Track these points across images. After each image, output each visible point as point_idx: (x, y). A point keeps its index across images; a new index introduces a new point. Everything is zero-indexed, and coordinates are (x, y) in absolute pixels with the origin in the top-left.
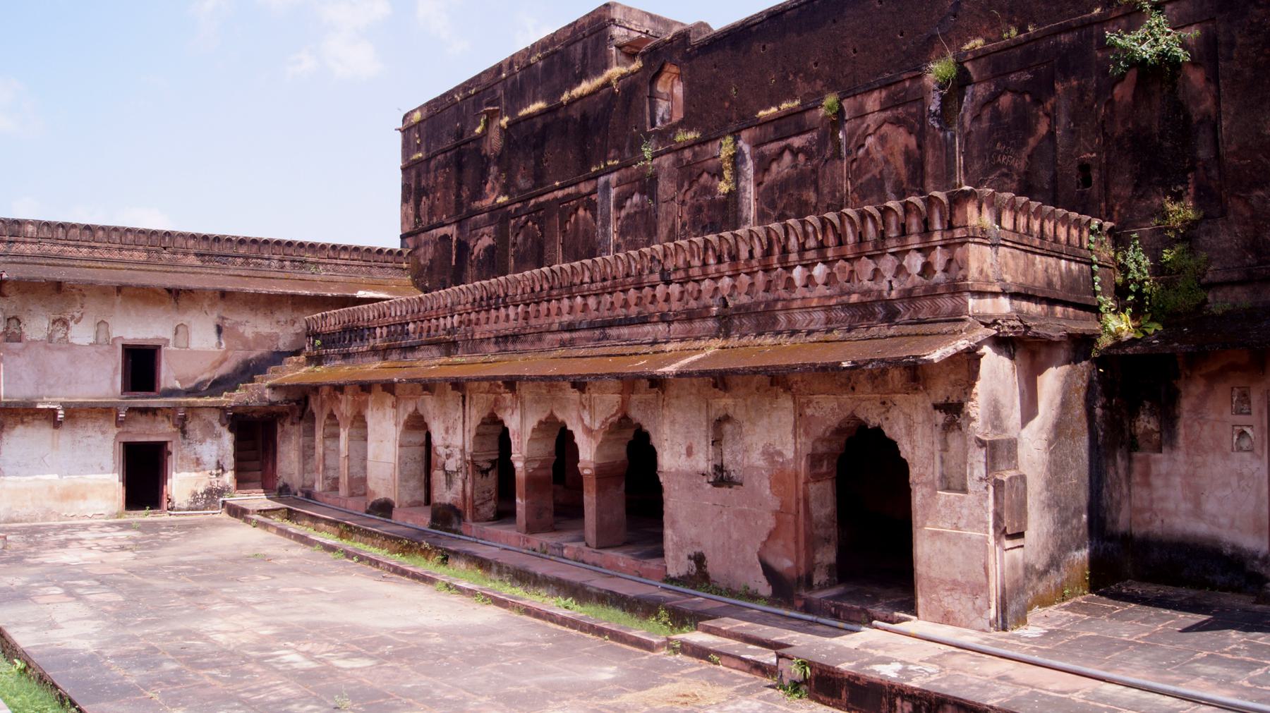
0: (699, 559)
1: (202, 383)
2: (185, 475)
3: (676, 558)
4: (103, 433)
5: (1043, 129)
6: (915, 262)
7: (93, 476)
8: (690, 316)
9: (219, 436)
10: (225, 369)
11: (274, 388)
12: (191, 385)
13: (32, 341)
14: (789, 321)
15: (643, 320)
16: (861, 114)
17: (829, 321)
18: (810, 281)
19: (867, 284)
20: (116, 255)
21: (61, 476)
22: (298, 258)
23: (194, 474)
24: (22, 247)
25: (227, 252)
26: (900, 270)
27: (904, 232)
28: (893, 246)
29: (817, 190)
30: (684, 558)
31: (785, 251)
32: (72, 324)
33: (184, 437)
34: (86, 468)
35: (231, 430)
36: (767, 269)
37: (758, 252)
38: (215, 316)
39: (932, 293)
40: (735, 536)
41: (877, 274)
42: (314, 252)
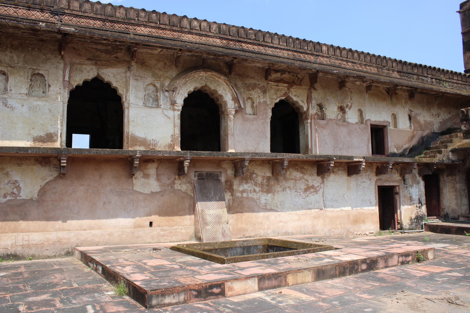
1: (405, 150)
2: (406, 207)
4: (370, 180)
7: (366, 208)
9: (418, 183)
10: (414, 142)
11: (453, 151)
12: (401, 151)
13: (331, 120)
20: (365, 70)
21: (352, 208)
22: (438, 78)
23: (410, 207)
24: (322, 59)
25: (410, 71)
32: (347, 110)
33: (405, 184)
34: (364, 203)
35: (423, 180)
38: (407, 109)
42: (444, 74)
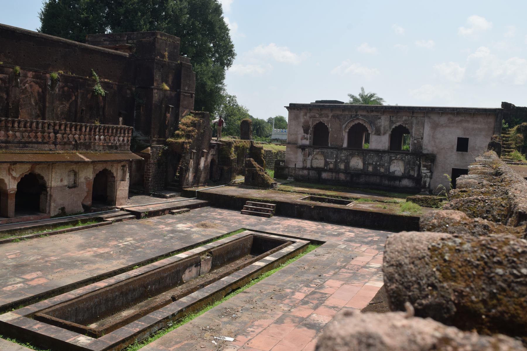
0: (63, 209)
3: (55, 211)
5: (74, 98)
6: (121, 139)
8: (65, 144)
14: (94, 147)
15: (47, 143)
16: (26, 76)
17: (103, 149)
18: (100, 139)
19: (112, 141)
26: (119, 140)
27: (120, 133)
28: (118, 135)
29: (8, 94)
30: (57, 210)
31: (95, 132)
36: (90, 134)
37: (88, 129)
39: (125, 145)
40: (75, 200)
41: (114, 140)
